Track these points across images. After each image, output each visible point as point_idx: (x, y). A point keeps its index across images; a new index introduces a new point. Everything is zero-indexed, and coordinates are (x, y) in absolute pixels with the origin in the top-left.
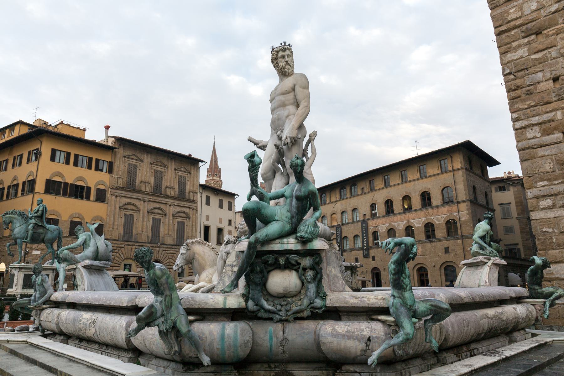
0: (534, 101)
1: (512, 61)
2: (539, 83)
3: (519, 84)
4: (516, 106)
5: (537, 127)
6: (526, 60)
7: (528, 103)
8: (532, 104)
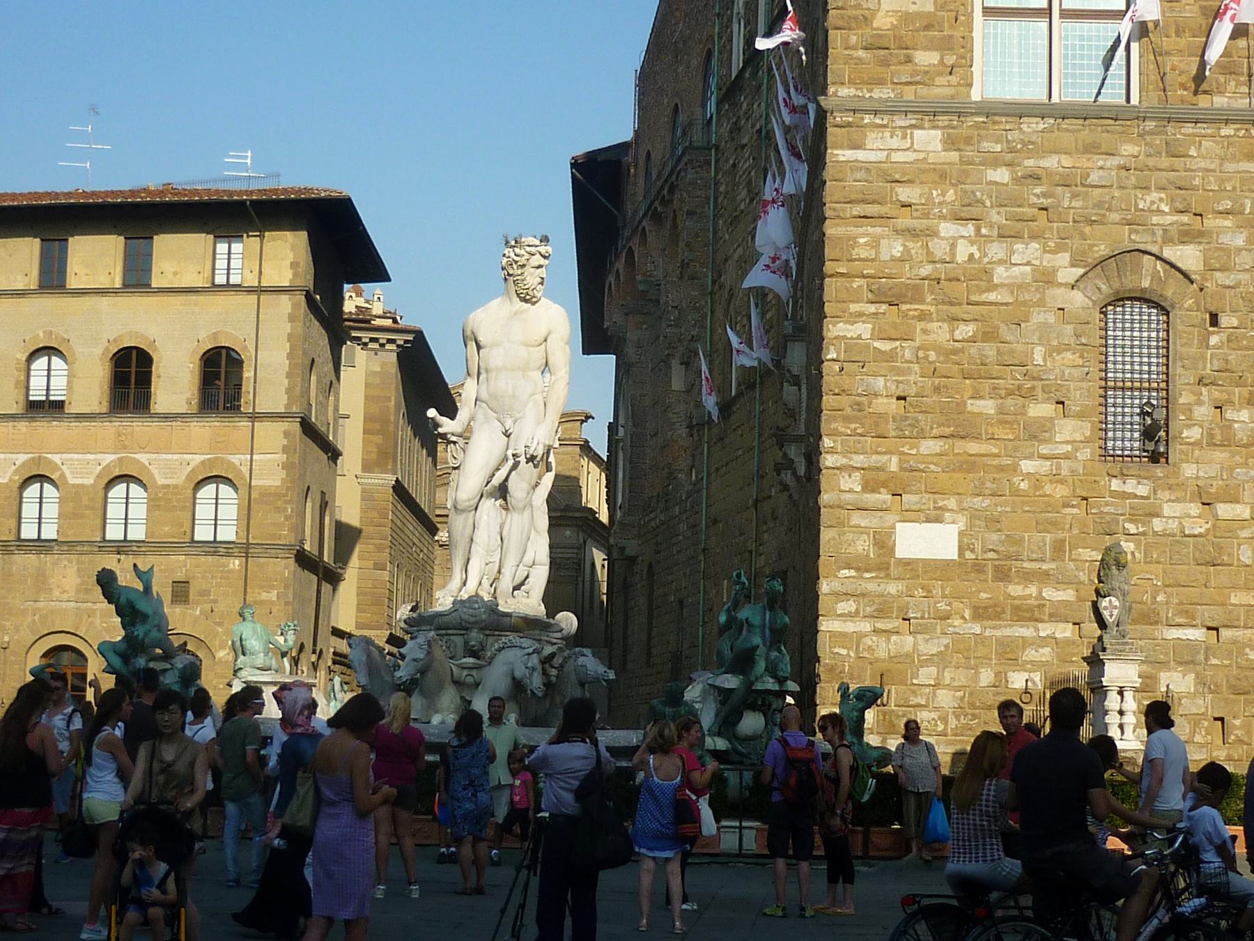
0: (863, 425)
1: (845, 337)
2: (876, 395)
3: (846, 387)
4: (833, 426)
5: (857, 475)
6: (867, 346)
7: (853, 426)
8: (858, 431)
